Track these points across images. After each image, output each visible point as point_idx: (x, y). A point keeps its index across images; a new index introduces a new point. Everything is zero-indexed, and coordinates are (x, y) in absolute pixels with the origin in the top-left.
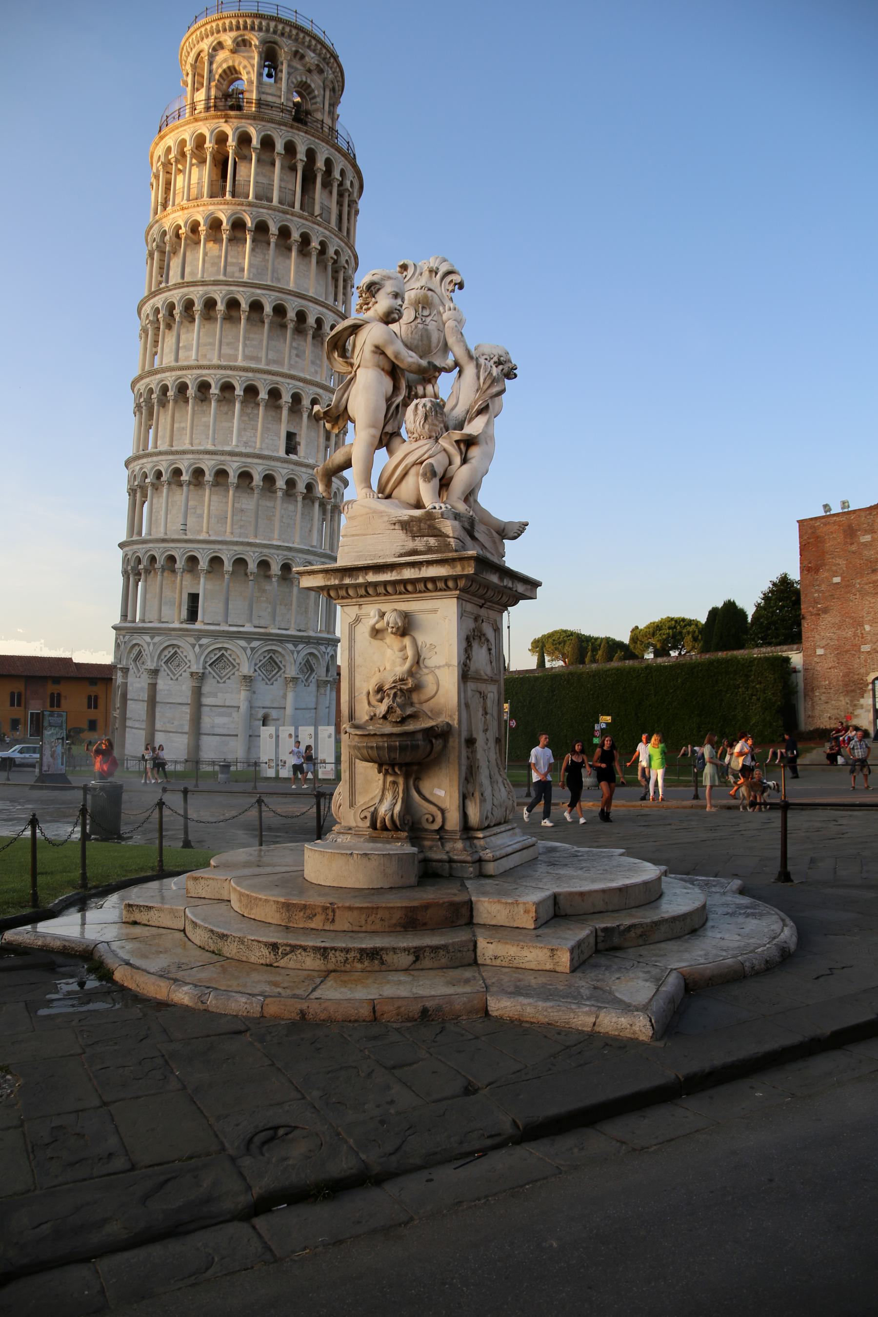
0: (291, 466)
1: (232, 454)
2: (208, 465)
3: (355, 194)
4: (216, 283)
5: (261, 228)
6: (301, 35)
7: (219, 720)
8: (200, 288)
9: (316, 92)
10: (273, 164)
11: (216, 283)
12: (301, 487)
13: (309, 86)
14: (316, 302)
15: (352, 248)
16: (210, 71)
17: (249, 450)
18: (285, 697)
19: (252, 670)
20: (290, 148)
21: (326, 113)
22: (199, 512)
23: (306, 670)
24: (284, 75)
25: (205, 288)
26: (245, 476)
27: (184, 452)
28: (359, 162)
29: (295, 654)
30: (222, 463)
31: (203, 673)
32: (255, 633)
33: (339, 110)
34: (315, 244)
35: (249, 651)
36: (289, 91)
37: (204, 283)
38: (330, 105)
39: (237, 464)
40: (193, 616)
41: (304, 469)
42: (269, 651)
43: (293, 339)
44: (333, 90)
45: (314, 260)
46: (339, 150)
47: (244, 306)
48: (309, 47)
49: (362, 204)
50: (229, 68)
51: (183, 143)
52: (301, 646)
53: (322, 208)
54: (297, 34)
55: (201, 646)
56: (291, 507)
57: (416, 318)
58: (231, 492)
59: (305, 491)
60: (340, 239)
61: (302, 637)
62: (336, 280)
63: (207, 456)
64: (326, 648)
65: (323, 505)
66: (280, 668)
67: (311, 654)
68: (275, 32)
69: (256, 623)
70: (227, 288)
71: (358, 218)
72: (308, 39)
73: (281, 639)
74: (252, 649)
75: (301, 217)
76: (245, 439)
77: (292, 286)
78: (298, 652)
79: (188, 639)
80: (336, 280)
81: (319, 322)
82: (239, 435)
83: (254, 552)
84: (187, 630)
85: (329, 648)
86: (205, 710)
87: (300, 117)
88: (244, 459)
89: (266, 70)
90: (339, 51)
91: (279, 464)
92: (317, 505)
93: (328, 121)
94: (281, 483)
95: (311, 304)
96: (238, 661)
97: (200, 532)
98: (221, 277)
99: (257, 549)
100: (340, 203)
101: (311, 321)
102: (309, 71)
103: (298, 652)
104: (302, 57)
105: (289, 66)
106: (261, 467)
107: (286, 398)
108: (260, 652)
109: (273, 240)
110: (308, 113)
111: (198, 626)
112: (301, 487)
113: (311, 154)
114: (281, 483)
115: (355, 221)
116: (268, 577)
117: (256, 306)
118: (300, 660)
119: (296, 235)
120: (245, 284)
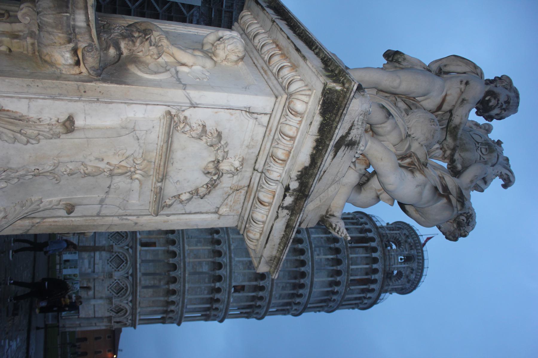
0: (227, 290)
1: (230, 257)
2: (223, 248)
3: (361, 306)
4: (310, 243)
5: (338, 262)
6: (420, 271)
7: (86, 262)
8: (306, 236)
9: (399, 281)
10: (367, 264)
11: (310, 243)
12: (217, 296)
13: (401, 278)
14: (310, 293)
15: (337, 308)
16: (396, 234)
17: (233, 267)
18: (101, 298)
19: (115, 278)
20: (375, 271)
21: (392, 287)
22: (199, 244)
23: (117, 309)
24: (403, 265)
25: (307, 238)
26: (220, 266)
27: (228, 235)
28: (375, 306)
29: (126, 302)
30: (225, 253)
31: (113, 252)
32: (136, 278)
33: (395, 295)
34: (336, 289)
35: (126, 275)
36: (398, 268)
37: (309, 237)
38: (396, 288)
39: (225, 261)
40: (143, 245)
41: (227, 296)
42: (127, 287)
43: (290, 283)
44: (402, 289)
45: (329, 289)
46: (379, 295)
47: (302, 258)
48: (416, 275)
49: (356, 310)
50: (400, 241)
51: (366, 224)
52: (130, 304)
53: (353, 290)
54: (420, 269)
55: (128, 249)
56: (206, 292)
57: (478, 143)
58: (211, 260)
59: (215, 298)
60: (341, 301)
61: (136, 304)
62: (321, 301)
63: (227, 246)
64: (130, 320)
65: (208, 309)
66: (117, 294)
67: (127, 311)
68: (418, 259)
69: (142, 279)
70: (309, 248)
71: (351, 310)
72: (419, 274)
73: (134, 293)
74: (127, 277)
75: (347, 279)
76: (238, 265)
77: (315, 280)
78: (127, 303)
79: (131, 242)
80: (321, 301)
81: (301, 296)
82: (239, 262)
83: (180, 274)
84: (136, 241)
85: (130, 321)
86: (92, 254)
87: (388, 275)
88: (228, 264)
89: (403, 257)
90: (418, 289)
91: (228, 282)
92: (208, 306)
93: (390, 287)
94: (218, 285)
95: (308, 290)
96: (121, 270)
97: (188, 245)
98: (313, 246)
99: (182, 276)
100: (356, 299)
101: (301, 291)
102: (407, 277)
103: (127, 303)
104: (412, 273)
105: (407, 267)
106: (225, 274)
107: (262, 283)
108: (126, 282)
109: (335, 268)
110: (390, 278)
111: (139, 247)
112: (217, 296)
113: (375, 281)
114: (218, 285)
115: (349, 308)
116: (168, 283)
117: (303, 263)
118: (123, 305)
119: (338, 279)
120: (312, 257)
